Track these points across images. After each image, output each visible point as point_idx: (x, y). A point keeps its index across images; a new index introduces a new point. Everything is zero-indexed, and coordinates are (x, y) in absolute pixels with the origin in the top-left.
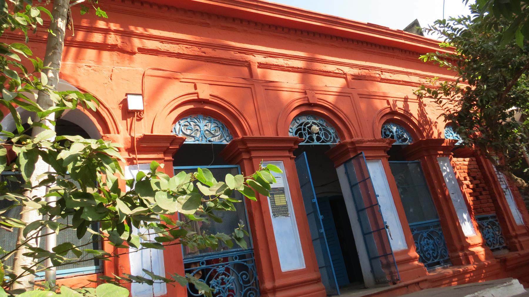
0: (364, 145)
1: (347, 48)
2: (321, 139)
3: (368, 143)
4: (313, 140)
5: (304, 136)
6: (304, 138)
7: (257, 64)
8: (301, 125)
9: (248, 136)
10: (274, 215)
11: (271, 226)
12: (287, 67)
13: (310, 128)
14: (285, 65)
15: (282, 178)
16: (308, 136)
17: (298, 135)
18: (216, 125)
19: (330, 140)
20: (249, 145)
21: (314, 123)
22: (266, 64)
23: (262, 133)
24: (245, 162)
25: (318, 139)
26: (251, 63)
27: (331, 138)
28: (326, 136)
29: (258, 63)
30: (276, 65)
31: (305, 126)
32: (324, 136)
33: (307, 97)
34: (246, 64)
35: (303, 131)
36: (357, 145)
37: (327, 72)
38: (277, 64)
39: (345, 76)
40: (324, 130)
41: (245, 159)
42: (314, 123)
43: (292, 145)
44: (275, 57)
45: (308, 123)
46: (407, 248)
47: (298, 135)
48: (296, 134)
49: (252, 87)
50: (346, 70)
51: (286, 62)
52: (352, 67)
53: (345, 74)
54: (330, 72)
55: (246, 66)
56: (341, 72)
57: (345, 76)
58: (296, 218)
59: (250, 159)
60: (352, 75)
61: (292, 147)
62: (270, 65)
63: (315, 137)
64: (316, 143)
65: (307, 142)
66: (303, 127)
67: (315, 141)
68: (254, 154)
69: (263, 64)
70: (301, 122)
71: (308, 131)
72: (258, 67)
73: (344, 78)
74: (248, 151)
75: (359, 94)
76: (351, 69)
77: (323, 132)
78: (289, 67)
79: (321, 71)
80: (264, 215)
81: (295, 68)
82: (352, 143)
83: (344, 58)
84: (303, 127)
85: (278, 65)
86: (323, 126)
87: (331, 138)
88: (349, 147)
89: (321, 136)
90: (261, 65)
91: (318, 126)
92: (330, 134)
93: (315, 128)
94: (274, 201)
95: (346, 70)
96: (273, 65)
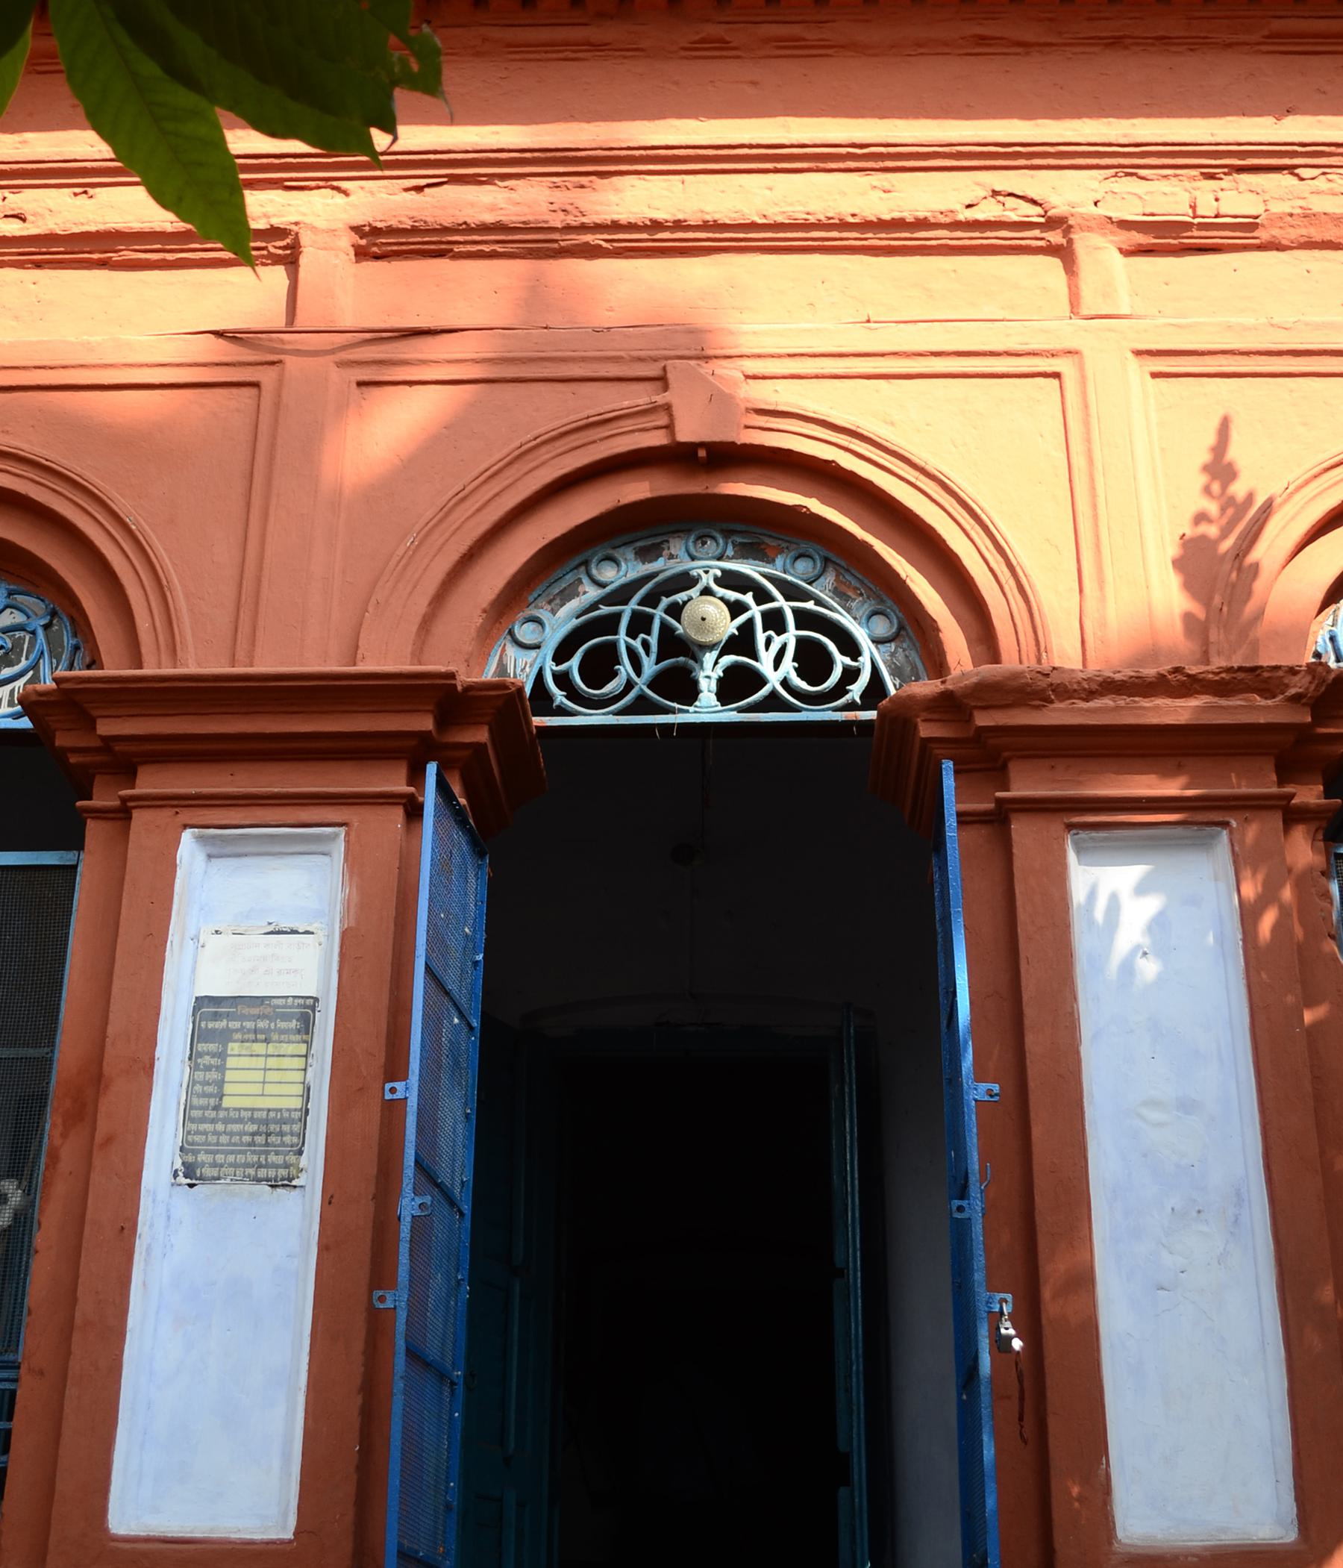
0: (1058, 714)
1: (1115, 43)
2: (760, 681)
3: (1107, 702)
4: (689, 693)
5: (625, 668)
6: (612, 687)
7: (346, 242)
8: (622, 595)
9: (147, 671)
10: (191, 1174)
11: (126, 1231)
12: (568, 229)
13: (676, 610)
14: (557, 221)
15: (320, 935)
16: (650, 666)
17: (574, 663)
18: (19, 618)
19: (840, 690)
20: (106, 728)
21: (730, 580)
22: (414, 231)
23: (241, 654)
24: (94, 830)
25: (738, 683)
26: (305, 239)
27: (851, 675)
28: (812, 661)
29: (356, 229)
30: (484, 228)
31: (651, 600)
32: (788, 665)
33: (667, 408)
34: (274, 247)
35: (622, 637)
36: (982, 720)
37: (898, 224)
38: (489, 218)
39: (1055, 237)
40: (804, 619)
41: (100, 814)
42: (730, 580)
43: (425, 723)
44: (490, 180)
45: (686, 581)
46: (1288, 1534)
47: (574, 663)
48: (562, 654)
49: (266, 377)
50: (1067, 191)
51: (561, 198)
52: (1130, 172)
53: (1054, 223)
54: (922, 224)
55: (276, 260)
56: (1032, 213)
57: (1055, 237)
58: (328, 1200)
59: (122, 814)
60: (1125, 225)
61: (422, 736)
62: (445, 230)
63: (709, 673)
64: (709, 708)
65: (642, 705)
66: (633, 605)
67: (708, 695)
68: (149, 782)
69: (391, 231)
70: (612, 575)
71: (666, 630)
72: (362, 254)
73: (1051, 250)
74: (124, 761)
75: (1138, 353)
76: (1127, 185)
77: (791, 636)
78: (583, 228)
79: (843, 225)
80: (97, 1161)
81: (631, 227)
82: (951, 705)
83: (1078, 115)
84: (627, 611)
85: (499, 227)
86: (806, 596)
87: (851, 675)
88: (925, 731)
89: (764, 664)
90: (376, 244)
91: (762, 596)
92: (850, 647)
93: (711, 617)
94: (220, 1084)
95: (1067, 191)
96: (466, 229)
